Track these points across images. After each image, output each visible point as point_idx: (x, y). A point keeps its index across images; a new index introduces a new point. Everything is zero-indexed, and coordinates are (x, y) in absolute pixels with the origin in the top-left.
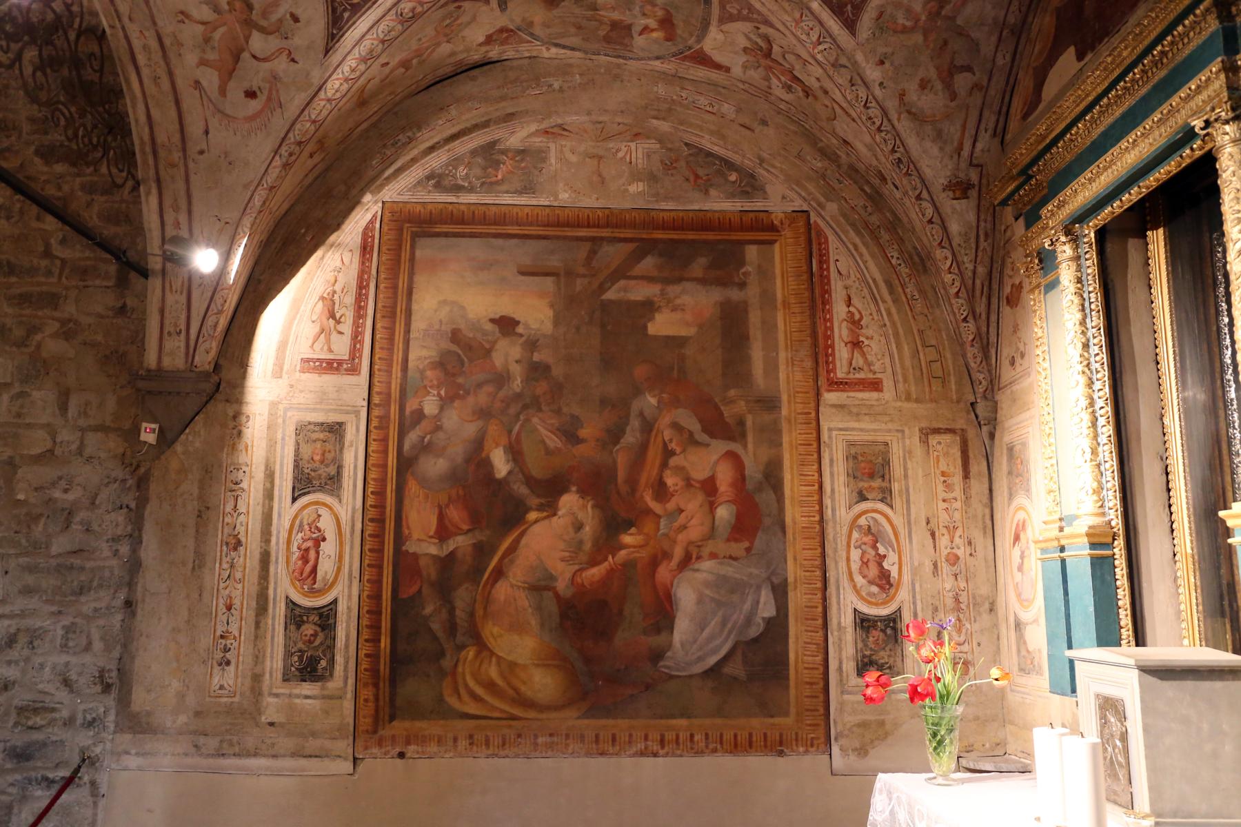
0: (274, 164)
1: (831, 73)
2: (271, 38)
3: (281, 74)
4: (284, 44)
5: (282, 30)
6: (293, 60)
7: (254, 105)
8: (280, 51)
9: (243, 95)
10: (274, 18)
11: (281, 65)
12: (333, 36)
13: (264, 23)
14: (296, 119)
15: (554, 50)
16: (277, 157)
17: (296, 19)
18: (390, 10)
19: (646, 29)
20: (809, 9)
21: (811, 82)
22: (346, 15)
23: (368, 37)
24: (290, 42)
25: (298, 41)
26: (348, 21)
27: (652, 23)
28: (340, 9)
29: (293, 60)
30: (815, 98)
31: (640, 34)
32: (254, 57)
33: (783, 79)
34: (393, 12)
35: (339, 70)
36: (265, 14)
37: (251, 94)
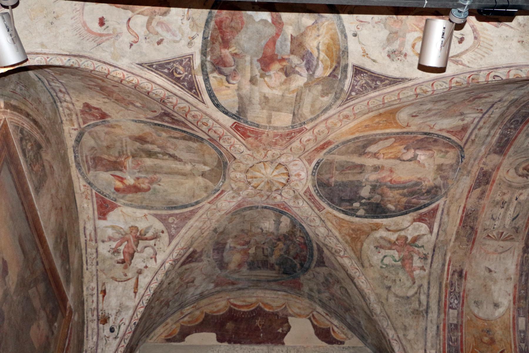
0: (63, 58)
1: (160, 272)
2: (145, 29)
3: (121, 39)
4: (141, 38)
5: (151, 35)
6: (131, 45)
7: (95, 27)
8: (137, 36)
9: (100, 16)
10: (159, 29)
11: (126, 38)
12: (151, 65)
13: (154, 23)
14: (93, 59)
15: (75, 133)
16: (68, 58)
17: (159, 43)
18: (171, 92)
19: (121, 179)
20: (189, 248)
21: (138, 262)
22: (166, 71)
23: (154, 85)
24: (144, 41)
25: (144, 45)
26: (162, 72)
27: (130, 181)
28: (169, 66)
29: (131, 45)
30: (126, 268)
31: (112, 175)
32: (129, 20)
33: (122, 248)
34: (170, 94)
35: (130, 75)
36: (160, 23)
37: (102, 22)
